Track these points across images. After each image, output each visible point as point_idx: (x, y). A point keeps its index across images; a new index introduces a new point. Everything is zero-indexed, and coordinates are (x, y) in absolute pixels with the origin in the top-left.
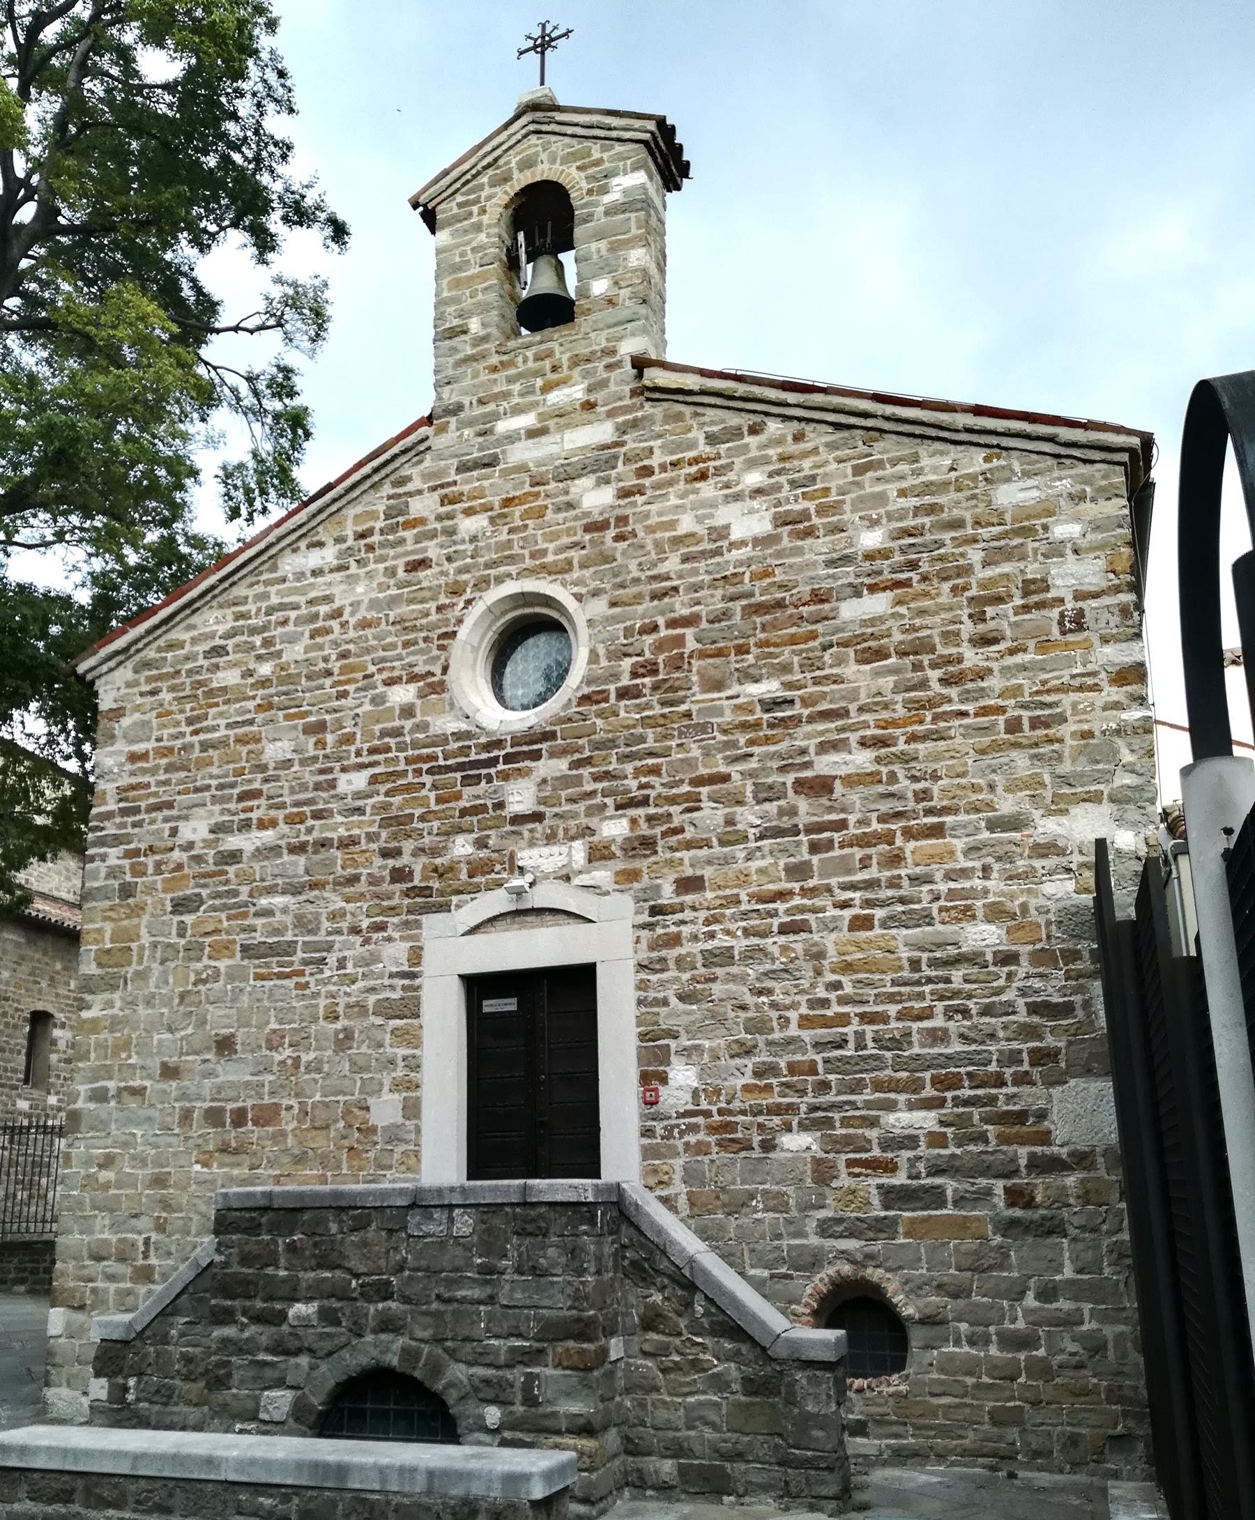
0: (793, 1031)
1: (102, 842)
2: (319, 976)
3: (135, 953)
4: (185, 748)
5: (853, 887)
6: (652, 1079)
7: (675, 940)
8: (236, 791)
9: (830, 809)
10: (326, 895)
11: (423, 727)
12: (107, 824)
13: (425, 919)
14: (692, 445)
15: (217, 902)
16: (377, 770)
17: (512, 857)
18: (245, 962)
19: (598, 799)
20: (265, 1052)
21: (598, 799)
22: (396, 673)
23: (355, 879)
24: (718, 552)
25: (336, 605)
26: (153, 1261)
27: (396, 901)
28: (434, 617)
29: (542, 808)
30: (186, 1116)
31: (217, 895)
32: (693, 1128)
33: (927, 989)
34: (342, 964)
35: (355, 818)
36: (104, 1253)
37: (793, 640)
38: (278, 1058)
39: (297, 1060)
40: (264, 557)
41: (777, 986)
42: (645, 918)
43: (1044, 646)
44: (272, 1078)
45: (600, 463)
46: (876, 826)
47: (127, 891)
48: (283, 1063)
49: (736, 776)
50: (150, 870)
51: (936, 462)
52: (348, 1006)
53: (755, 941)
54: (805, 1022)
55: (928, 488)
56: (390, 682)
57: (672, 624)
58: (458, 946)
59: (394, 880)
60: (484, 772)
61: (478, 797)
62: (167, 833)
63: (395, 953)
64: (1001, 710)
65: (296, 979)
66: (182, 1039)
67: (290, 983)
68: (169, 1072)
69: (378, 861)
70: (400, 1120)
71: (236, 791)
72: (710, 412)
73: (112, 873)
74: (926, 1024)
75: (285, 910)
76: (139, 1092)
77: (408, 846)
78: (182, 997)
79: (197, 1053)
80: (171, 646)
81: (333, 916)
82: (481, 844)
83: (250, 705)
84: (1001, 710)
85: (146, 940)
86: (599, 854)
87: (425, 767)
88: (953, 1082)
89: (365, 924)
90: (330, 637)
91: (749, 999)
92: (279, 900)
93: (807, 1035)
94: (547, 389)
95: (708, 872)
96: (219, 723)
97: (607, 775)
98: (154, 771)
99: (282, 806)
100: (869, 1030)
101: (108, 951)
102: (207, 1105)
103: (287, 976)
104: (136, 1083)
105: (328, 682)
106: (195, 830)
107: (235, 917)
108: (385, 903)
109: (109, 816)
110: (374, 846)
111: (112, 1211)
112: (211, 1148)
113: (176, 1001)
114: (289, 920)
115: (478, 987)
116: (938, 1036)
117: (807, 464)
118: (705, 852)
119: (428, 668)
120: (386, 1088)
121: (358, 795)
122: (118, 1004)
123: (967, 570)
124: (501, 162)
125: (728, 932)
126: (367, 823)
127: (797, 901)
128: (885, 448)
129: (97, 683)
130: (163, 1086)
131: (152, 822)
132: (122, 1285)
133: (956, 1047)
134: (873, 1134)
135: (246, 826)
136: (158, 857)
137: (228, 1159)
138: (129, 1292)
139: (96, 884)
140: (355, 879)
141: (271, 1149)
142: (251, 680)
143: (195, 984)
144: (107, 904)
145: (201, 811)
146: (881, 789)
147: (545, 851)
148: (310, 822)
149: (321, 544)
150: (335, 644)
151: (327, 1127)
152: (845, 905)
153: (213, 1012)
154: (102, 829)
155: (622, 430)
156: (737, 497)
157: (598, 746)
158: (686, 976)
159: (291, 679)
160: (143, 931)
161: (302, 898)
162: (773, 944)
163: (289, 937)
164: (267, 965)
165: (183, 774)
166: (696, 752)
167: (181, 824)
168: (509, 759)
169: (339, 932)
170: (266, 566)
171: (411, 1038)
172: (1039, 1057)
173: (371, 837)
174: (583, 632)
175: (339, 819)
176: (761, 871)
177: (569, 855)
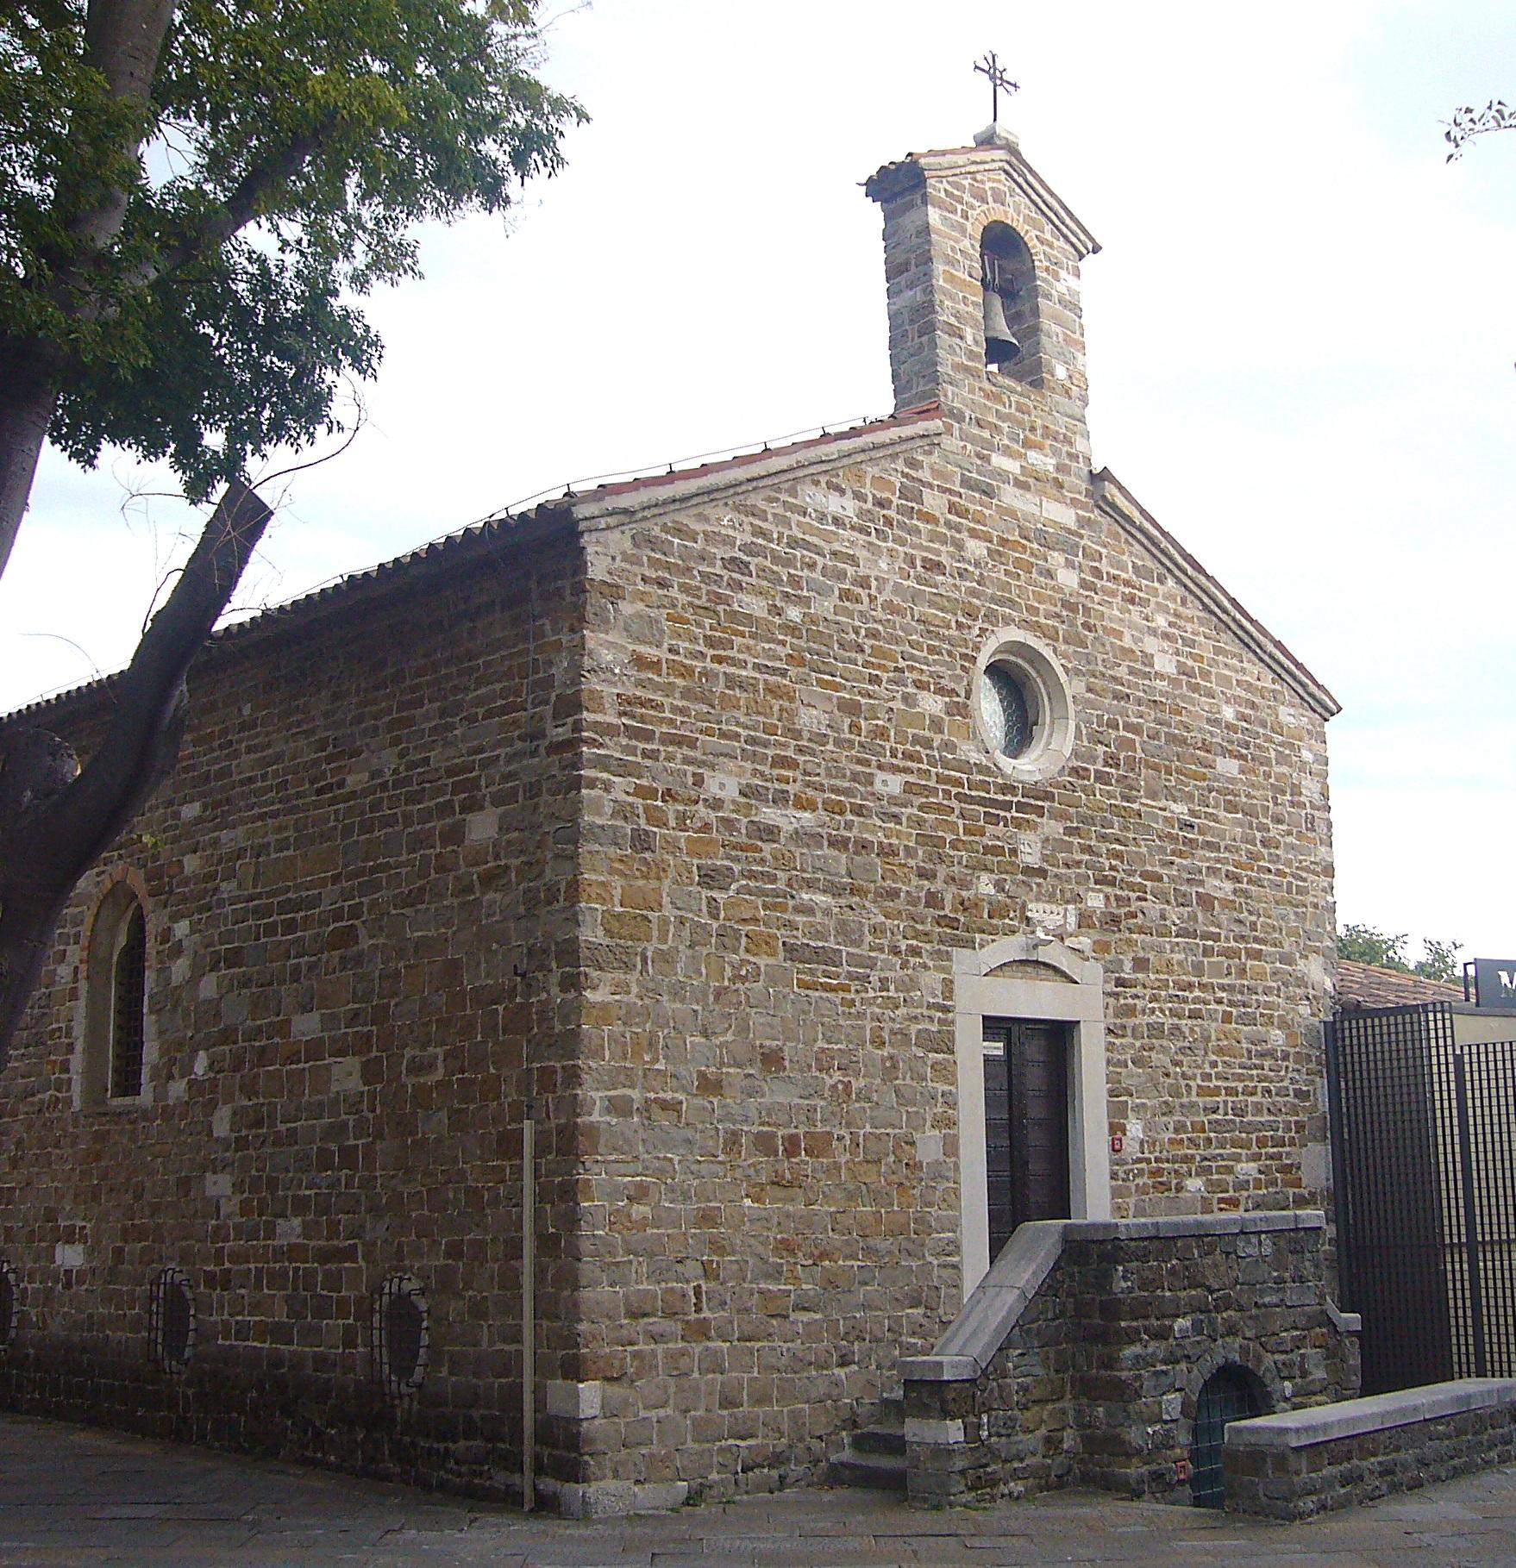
1: (602, 763)
2: (863, 995)
3: (654, 926)
4: (705, 673)
5: (1223, 988)
6: (1117, 1130)
7: (1130, 1011)
8: (770, 752)
9: (1213, 924)
10: (867, 904)
11: (949, 746)
13: (955, 951)
14: (1124, 569)
16: (911, 779)
17: (1024, 906)
18: (788, 964)
19: (1082, 870)
21: (1082, 870)
22: (925, 679)
23: (893, 894)
24: (1147, 676)
25: (862, 571)
26: (706, 1314)
27: (928, 928)
28: (954, 632)
29: (1045, 865)
30: (733, 1139)
31: (752, 876)
32: (1141, 1172)
33: (1254, 1072)
34: (884, 983)
35: (892, 825)
36: (648, 1308)
37: (1196, 776)
38: (830, 1082)
40: (790, 476)
41: (1185, 1060)
42: (1111, 987)
43: (1300, 835)
44: (823, 1103)
45: (1066, 542)
46: (1233, 944)
47: (642, 842)
48: (834, 1087)
49: (1166, 879)
50: (672, 823)
52: (893, 1032)
53: (1176, 1021)
54: (1202, 1091)
55: (1249, 687)
56: (920, 685)
57: (1127, 727)
58: (984, 986)
59: (927, 905)
60: (1002, 813)
61: (998, 838)
62: (690, 781)
63: (932, 979)
64: (1284, 875)
65: (841, 994)
66: (720, 1046)
67: (836, 997)
68: (710, 1085)
69: (915, 881)
70: (942, 1158)
71: (770, 752)
73: (623, 812)
74: (1254, 1099)
75: (827, 912)
77: (942, 871)
78: (718, 994)
80: (679, 531)
81: (874, 930)
82: (999, 885)
84: (1284, 875)
85: (669, 912)
86: (1084, 920)
87: (954, 791)
88: (1262, 1143)
90: (859, 607)
91: (1172, 1069)
92: (821, 899)
93: (1200, 1101)
94: (1027, 444)
95: (1151, 956)
96: (748, 657)
97: (1088, 850)
98: (668, 689)
99: (820, 788)
100: (1230, 1099)
102: (755, 1129)
103: (833, 989)
104: (668, 1096)
105: (860, 658)
106: (722, 786)
107: (775, 907)
108: (919, 927)
109: (610, 730)
110: (912, 863)
111: (652, 1255)
113: (711, 998)
115: (994, 1026)
116: (1258, 1108)
117: (1189, 627)
118: (1148, 938)
119: (953, 685)
120: (928, 1124)
121: (893, 800)
122: (635, 989)
123: (1268, 762)
124: (979, 177)
125: (1162, 1011)
126: (904, 836)
127: (1197, 993)
128: (1227, 641)
129: (586, 537)
130: (699, 1101)
131: (670, 758)
133: (1266, 1118)
134: (1230, 1178)
135: (781, 799)
136: (681, 808)
139: (599, 821)
140: (893, 894)
142: (777, 620)
143: (732, 980)
144: (613, 851)
145: (731, 765)
146: (1235, 914)
147: (1047, 907)
148: (850, 817)
149: (842, 492)
151: (879, 1161)
152: (1219, 1002)
153: (756, 1019)
155: (1084, 523)
156: (1153, 632)
157: (1084, 819)
158: (1138, 1044)
160: (666, 900)
161: (843, 902)
164: (812, 972)
165: (705, 709)
166: (1144, 850)
168: (1021, 807)
169: (881, 950)
170: (786, 486)
171: (946, 1072)
172: (1300, 1127)
173: (910, 852)
174: (1071, 707)
175: (879, 823)
176: (1180, 963)
177: (1065, 916)
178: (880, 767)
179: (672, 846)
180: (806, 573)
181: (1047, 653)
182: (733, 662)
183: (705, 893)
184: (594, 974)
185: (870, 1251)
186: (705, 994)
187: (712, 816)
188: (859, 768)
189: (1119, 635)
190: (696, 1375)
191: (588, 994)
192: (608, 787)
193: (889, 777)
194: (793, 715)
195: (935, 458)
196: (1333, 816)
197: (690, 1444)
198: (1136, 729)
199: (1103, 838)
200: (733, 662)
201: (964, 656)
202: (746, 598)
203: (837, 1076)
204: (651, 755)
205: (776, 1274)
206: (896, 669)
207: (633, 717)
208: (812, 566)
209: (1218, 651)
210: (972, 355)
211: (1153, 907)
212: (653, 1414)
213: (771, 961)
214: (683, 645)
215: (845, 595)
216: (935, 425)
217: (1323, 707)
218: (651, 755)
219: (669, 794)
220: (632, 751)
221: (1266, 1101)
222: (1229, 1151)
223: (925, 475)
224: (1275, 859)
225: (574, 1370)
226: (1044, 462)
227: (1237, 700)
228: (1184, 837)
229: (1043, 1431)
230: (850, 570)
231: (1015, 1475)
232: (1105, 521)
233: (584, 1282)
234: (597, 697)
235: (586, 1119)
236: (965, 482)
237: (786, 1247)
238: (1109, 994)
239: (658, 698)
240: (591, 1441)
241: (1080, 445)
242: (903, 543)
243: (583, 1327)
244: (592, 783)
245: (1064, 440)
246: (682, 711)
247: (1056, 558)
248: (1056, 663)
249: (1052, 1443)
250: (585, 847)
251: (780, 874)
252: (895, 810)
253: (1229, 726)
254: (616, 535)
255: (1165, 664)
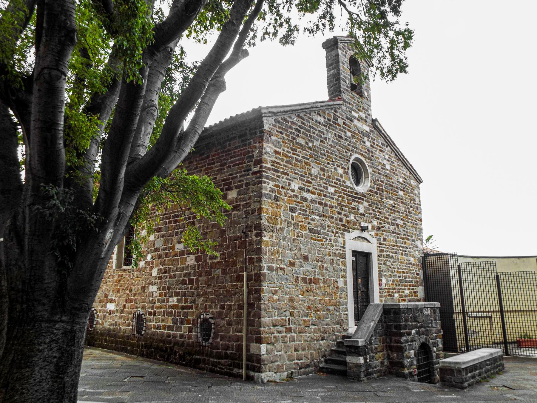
0: (396, 274)
1: (267, 177)
3: (279, 221)
4: (291, 157)
6: (380, 280)
8: (305, 179)
11: (344, 182)
12: (268, 171)
15: (301, 212)
16: (336, 189)
17: (360, 224)
20: (316, 262)
23: (332, 218)
24: (384, 169)
25: (325, 136)
26: (291, 326)
27: (340, 227)
28: (345, 154)
30: (297, 278)
31: (301, 210)
32: (385, 292)
34: (330, 239)
36: (277, 324)
38: (319, 265)
39: (323, 266)
40: (310, 110)
42: (378, 245)
43: (415, 211)
47: (276, 199)
50: (283, 195)
51: (406, 171)
54: (398, 272)
55: (405, 175)
56: (338, 166)
58: (352, 242)
59: (340, 221)
67: (320, 243)
69: (337, 215)
71: (305, 179)
72: (382, 138)
73: (272, 191)
75: (318, 221)
76: (283, 269)
77: (343, 213)
79: (298, 259)
81: (329, 226)
82: (355, 217)
83: (308, 154)
88: (410, 286)
89: (334, 231)
94: (359, 110)
95: (387, 238)
97: (373, 210)
98: (282, 160)
99: (316, 189)
101: (271, 218)
102: (302, 276)
103: (319, 241)
105: (325, 158)
106: (295, 186)
109: (269, 169)
110: (336, 210)
112: (304, 290)
114: (319, 224)
121: (332, 194)
122: (274, 238)
130: (289, 268)
131: (283, 178)
132: (283, 334)
133: (410, 279)
134: (404, 294)
135: (308, 191)
137: (308, 294)
138: (286, 336)
140: (332, 218)
141: (318, 291)
143: (298, 236)
144: (269, 200)
148: (323, 197)
149: (321, 116)
150: (325, 147)
151: (329, 286)
154: (267, 173)
155: (371, 131)
156: (385, 159)
157: (372, 203)
159: (315, 151)
160: (282, 214)
161: (321, 218)
162: (394, 255)
163: (319, 229)
164: (315, 236)
165: (291, 166)
167: (291, 182)
168: (360, 198)
171: (344, 264)
172: (417, 282)
174: (370, 175)
178: (329, 185)
179: (283, 201)
180: (313, 135)
181: (364, 161)
182: (297, 155)
183: (291, 214)
184: (265, 232)
185: (328, 310)
186: (291, 240)
187: (292, 194)
188: (325, 185)
189: (379, 159)
190: (288, 343)
191: (263, 238)
192: (268, 184)
193: (331, 188)
194: (310, 170)
195: (340, 111)
196: (421, 207)
197: (287, 362)
198: (382, 182)
199: (376, 208)
200: (297, 155)
201: (347, 160)
202: (300, 139)
203: (320, 263)
204: (279, 176)
205: (307, 315)
206: (333, 161)
207: (274, 166)
208: (314, 133)
209: (398, 165)
210: (347, 87)
211: (387, 226)
212: (279, 353)
213: (305, 232)
214: (286, 149)
215: (322, 142)
216: (341, 102)
217: (419, 181)
218: (279, 176)
219: (282, 187)
220: (274, 175)
221: (410, 275)
222: (403, 287)
223: (338, 114)
224: (411, 216)
225: (259, 341)
226: (363, 115)
227: (403, 177)
228: (393, 209)
229: (380, 360)
230: (323, 135)
231: (375, 372)
232: (375, 131)
233: (262, 316)
234: (266, 160)
235: (263, 271)
236: (347, 118)
237: (309, 308)
238: (378, 246)
239: (280, 162)
240: (264, 361)
241: (370, 112)
242: (334, 130)
243: (262, 329)
244: (265, 182)
245: (367, 110)
246: (286, 166)
247: (366, 139)
248: (366, 164)
249: (382, 363)
250: (264, 199)
251: (308, 210)
252: (333, 196)
253: (401, 184)
254: (270, 119)
255: (388, 167)
